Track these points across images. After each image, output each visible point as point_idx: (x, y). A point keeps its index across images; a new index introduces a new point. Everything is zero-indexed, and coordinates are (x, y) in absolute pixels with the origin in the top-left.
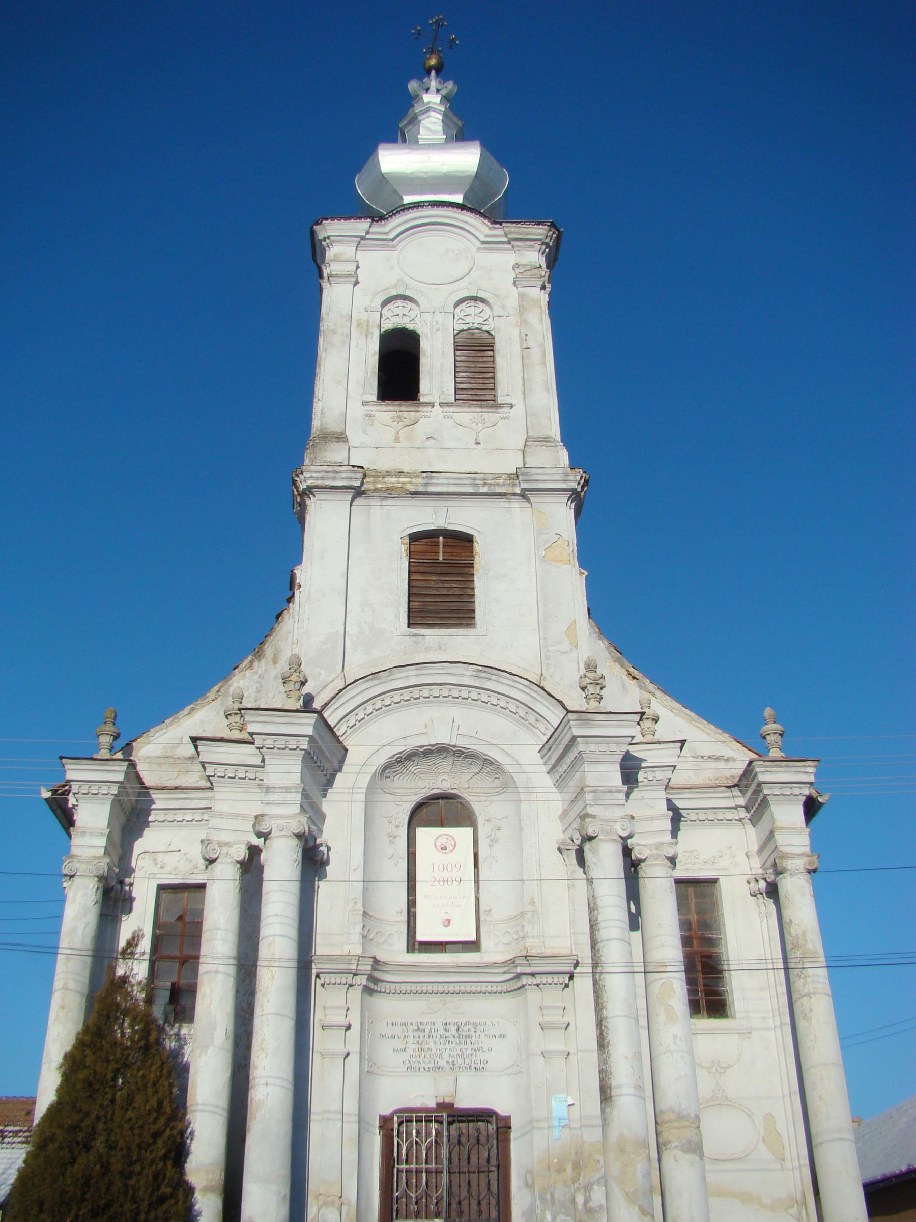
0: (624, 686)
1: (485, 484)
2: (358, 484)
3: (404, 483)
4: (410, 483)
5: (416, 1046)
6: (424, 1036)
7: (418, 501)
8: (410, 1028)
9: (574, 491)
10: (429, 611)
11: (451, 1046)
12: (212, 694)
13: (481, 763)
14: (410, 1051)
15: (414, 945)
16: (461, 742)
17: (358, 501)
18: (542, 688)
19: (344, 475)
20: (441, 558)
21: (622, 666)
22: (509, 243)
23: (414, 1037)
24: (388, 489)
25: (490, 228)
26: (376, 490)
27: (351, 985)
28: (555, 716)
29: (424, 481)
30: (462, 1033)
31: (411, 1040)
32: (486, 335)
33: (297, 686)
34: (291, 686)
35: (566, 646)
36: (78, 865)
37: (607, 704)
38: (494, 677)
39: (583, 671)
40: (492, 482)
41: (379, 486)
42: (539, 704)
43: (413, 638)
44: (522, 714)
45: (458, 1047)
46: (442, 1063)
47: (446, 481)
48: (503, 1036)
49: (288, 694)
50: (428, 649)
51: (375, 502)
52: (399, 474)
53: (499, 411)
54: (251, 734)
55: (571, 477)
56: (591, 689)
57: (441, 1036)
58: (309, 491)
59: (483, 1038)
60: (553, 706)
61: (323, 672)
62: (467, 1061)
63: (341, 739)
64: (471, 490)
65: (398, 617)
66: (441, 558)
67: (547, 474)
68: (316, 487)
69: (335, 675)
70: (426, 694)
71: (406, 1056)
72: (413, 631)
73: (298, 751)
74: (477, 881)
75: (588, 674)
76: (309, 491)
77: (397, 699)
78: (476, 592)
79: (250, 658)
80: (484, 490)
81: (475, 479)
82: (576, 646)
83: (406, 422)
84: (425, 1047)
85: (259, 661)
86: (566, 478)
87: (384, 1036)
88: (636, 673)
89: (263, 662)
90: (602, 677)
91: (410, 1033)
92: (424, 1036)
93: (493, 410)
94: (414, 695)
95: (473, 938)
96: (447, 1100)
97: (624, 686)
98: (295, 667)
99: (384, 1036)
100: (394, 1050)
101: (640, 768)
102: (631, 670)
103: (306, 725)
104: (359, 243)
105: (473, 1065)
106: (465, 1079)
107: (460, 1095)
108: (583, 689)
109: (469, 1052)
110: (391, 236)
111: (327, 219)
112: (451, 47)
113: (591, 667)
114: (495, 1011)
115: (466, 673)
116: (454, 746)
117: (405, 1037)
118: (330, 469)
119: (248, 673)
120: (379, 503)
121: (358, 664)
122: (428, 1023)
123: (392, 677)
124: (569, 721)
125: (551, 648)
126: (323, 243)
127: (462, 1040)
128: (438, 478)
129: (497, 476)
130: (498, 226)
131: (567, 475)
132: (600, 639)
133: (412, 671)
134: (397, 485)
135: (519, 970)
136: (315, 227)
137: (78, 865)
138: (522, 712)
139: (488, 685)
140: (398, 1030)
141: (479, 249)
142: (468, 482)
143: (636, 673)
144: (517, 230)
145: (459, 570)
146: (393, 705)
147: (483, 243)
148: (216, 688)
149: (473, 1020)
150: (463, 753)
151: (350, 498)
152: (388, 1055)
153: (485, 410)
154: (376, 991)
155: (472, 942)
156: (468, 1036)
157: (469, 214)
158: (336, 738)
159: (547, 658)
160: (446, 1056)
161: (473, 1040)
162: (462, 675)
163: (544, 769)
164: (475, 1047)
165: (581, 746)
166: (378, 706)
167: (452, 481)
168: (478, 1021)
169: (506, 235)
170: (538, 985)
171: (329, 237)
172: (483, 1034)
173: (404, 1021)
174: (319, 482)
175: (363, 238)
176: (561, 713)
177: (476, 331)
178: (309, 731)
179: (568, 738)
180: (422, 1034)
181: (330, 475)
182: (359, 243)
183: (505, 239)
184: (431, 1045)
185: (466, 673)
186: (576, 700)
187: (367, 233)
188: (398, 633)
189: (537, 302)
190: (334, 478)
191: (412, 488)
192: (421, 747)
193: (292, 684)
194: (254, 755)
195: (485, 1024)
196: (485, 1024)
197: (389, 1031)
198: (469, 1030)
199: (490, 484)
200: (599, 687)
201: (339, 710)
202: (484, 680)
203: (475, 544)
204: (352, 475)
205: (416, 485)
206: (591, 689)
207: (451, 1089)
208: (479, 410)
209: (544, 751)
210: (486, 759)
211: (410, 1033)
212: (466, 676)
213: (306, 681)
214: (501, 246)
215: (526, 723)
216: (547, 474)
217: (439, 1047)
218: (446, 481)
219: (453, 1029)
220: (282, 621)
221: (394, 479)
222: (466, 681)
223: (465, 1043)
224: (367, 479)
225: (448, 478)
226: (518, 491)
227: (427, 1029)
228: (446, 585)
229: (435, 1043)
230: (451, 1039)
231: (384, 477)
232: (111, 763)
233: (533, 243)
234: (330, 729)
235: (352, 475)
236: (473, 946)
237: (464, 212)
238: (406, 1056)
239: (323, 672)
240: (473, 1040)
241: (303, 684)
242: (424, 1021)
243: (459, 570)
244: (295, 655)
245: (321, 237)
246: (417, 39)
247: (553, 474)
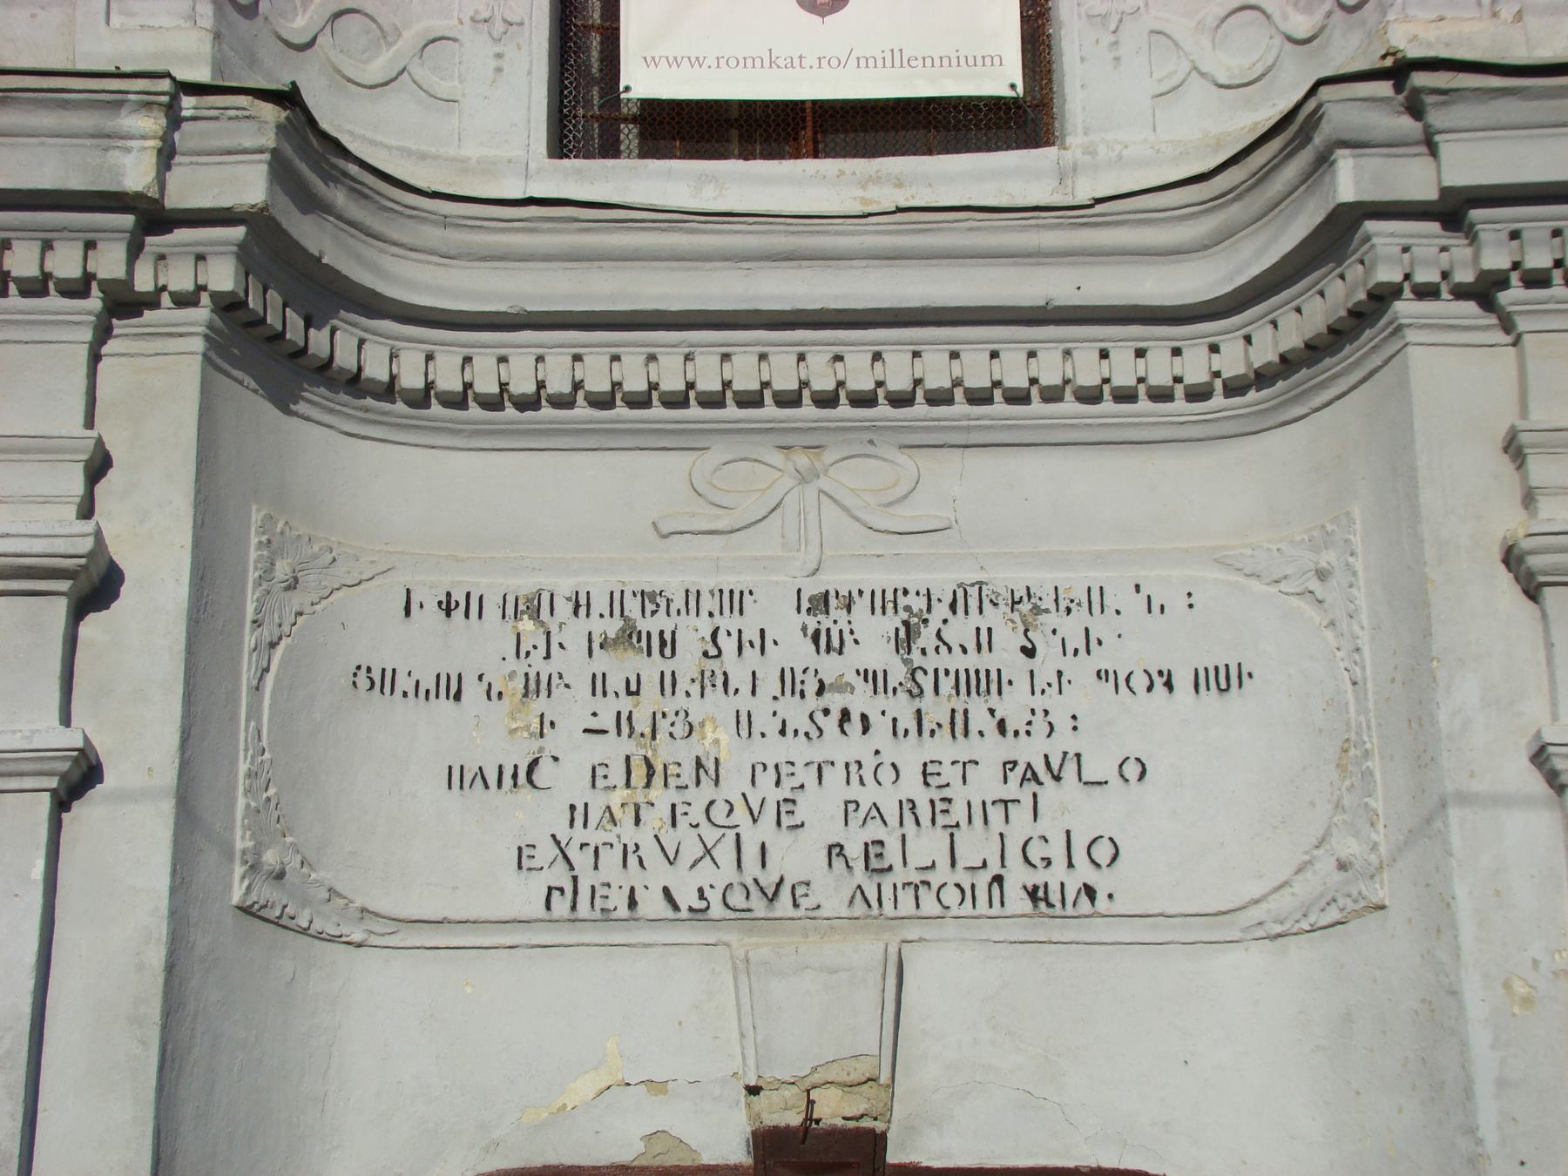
5: (613, 749)
6: (668, 684)
8: (573, 633)
11: (854, 746)
14: (566, 781)
15: (589, 108)
23: (598, 686)
27: (125, 303)
30: (938, 656)
31: (573, 708)
45: (910, 754)
46: (797, 858)
48: (1222, 680)
57: (789, 682)
59: (1084, 695)
62: (976, 845)
71: (537, 816)
84: (672, 752)
87: (384, 682)
91: (573, 663)
92: (668, 684)
95: (1002, 76)
96: (833, 1109)
99: (384, 682)
100: (456, 778)
105: (1018, 877)
106: (954, 977)
107: (922, 1076)
109: (986, 784)
114: (1169, 530)
117: (533, 687)
122: (692, 598)
127: (936, 710)
135: (1349, 181)
140: (484, 647)
149: (1006, 578)
152: (414, 818)
154: (324, 371)
155: (996, 105)
156: (976, 683)
160: (821, 810)
161: (1013, 706)
164: (1030, 751)
168: (1042, 580)
170: (1484, 291)
172: (1081, 670)
173: (524, 585)
180: (650, 668)
184: (719, 739)
195: (1096, 600)
196: (1096, 600)
197: (422, 648)
198: (984, 641)
207: (856, 1032)
211: (573, 663)
217: (775, 750)
219: (872, 640)
223: (959, 725)
227: (692, 633)
229: (744, 723)
230: (860, 700)
236: (1020, 120)
238: (537, 816)
240: (1013, 706)
242: (673, 584)
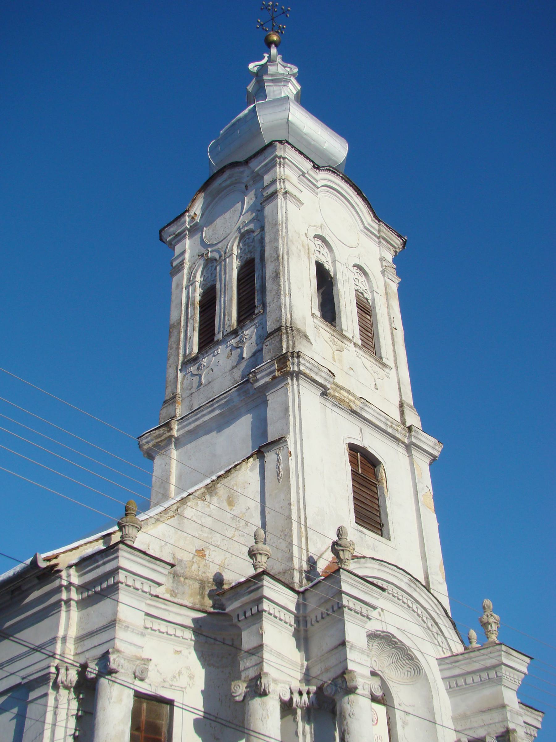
1: (391, 427)
4: (354, 402)
9: (435, 457)
19: (323, 375)
22: (378, 238)
25: (372, 220)
26: (334, 397)
29: (362, 405)
32: (365, 301)
36: (122, 661)
38: (418, 589)
40: (395, 427)
41: (337, 394)
51: (329, 405)
52: (349, 392)
53: (384, 369)
64: (383, 427)
76: (298, 374)
80: (390, 430)
81: (387, 419)
85: (211, 496)
86: (434, 446)
93: (381, 366)
115: (404, 579)
120: (330, 407)
128: (369, 407)
130: (377, 221)
131: (435, 444)
133: (375, 565)
134: (346, 400)
137: (122, 661)
141: (361, 230)
142: (383, 420)
144: (387, 232)
145: (369, 486)
147: (365, 228)
157: (361, 200)
162: (402, 580)
167: (375, 414)
169: (379, 231)
171: (284, 158)
174: (307, 372)
177: (360, 295)
181: (315, 369)
185: (404, 579)
190: (317, 374)
191: (354, 408)
199: (394, 428)
204: (328, 377)
205: (356, 405)
208: (374, 361)
212: (403, 582)
214: (373, 236)
221: (346, 394)
225: (374, 410)
226: (406, 441)
232: (158, 562)
233: (391, 247)
235: (328, 377)
237: (358, 196)
243: (369, 486)
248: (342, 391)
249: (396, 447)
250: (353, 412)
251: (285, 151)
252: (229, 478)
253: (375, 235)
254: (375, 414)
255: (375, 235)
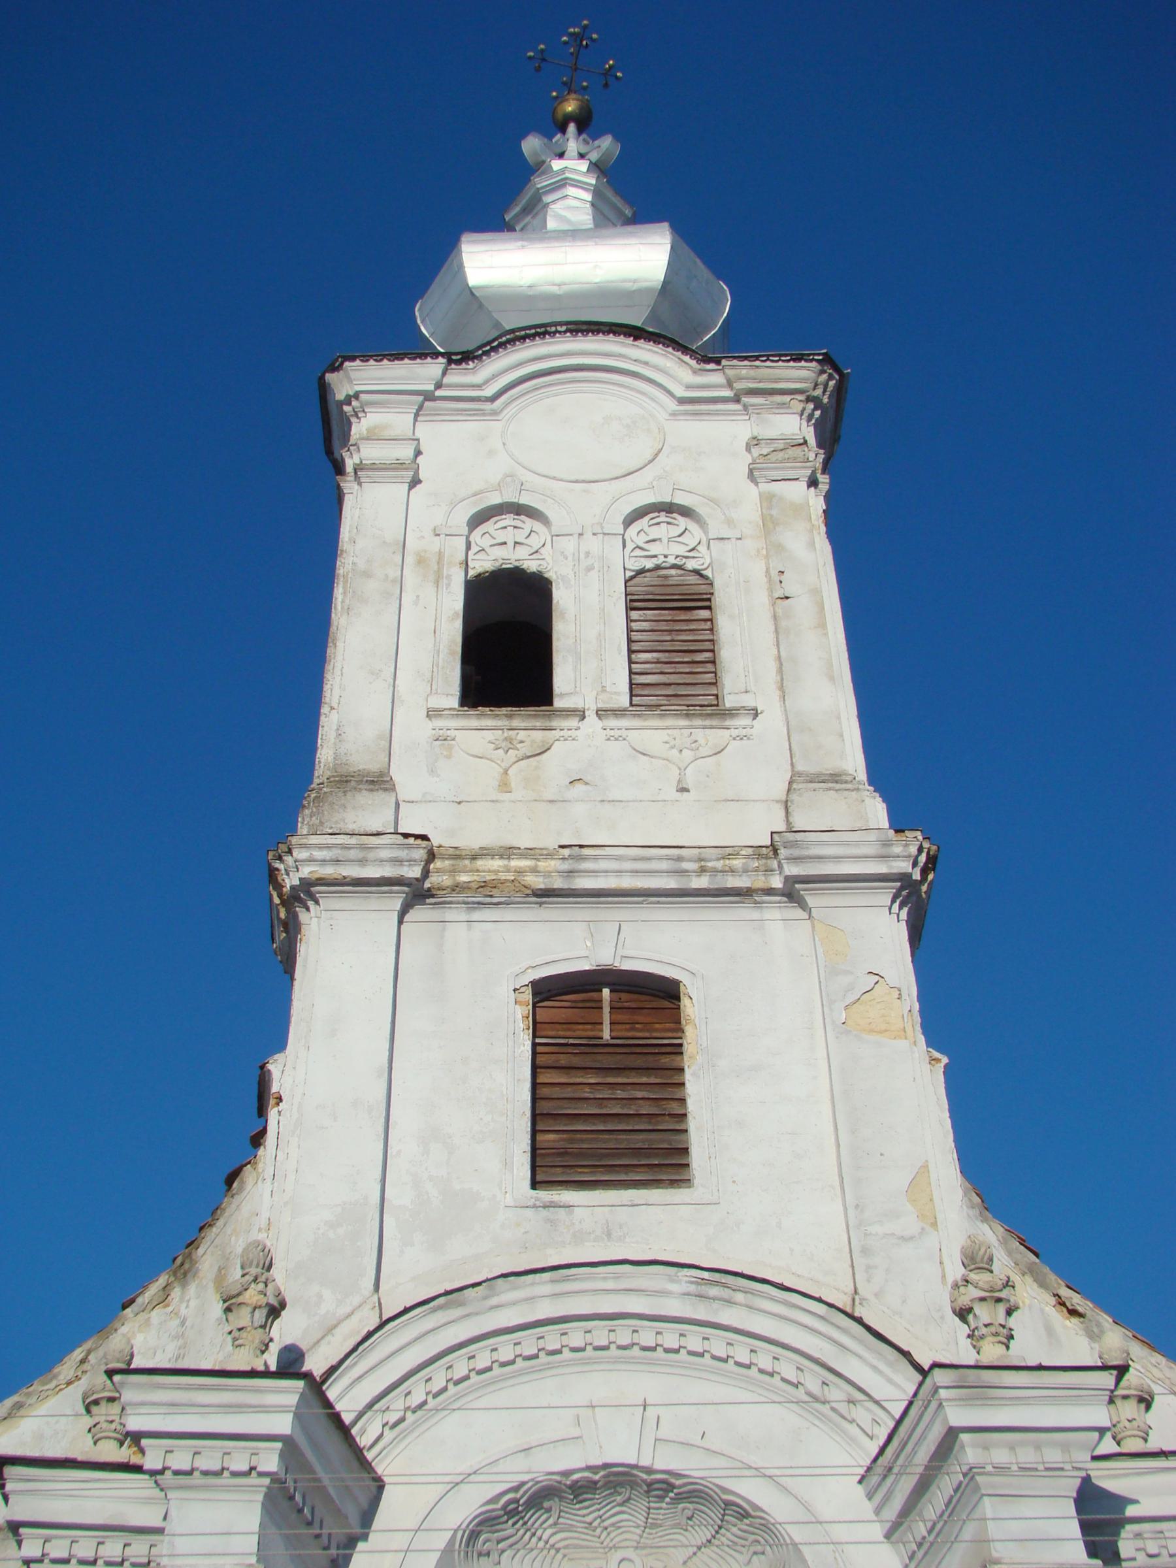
0: (1050, 1331)
1: (703, 870)
2: (415, 872)
3: (520, 872)
4: (534, 870)
7: (553, 912)
9: (904, 878)
10: (582, 1154)
12: (66, 1369)
13: (715, 1515)
16: (665, 1461)
17: (415, 914)
18: (859, 1321)
19: (385, 854)
20: (606, 1035)
21: (1042, 1284)
22: (736, 399)
24: (484, 885)
25: (695, 372)
26: (457, 888)
28: (894, 1386)
29: (566, 866)
32: (693, 579)
33: (260, 1316)
34: (243, 1317)
35: (909, 1222)
37: (1026, 1349)
38: (739, 1297)
39: (956, 1271)
40: (719, 865)
41: (464, 878)
42: (855, 1362)
43: (544, 1213)
44: (813, 1385)
47: (614, 865)
49: (236, 1336)
50: (579, 1238)
52: (508, 852)
53: (728, 723)
54: (136, 1438)
55: (897, 850)
56: (983, 1313)
58: (306, 892)
60: (890, 1364)
61: (327, 1294)
63: (369, 1456)
64: (671, 883)
65: (507, 1164)
66: (606, 1035)
67: (847, 843)
68: (321, 882)
69: (356, 1300)
70: (576, 1340)
72: (544, 1195)
73: (253, 1480)
74: (853, 1267)
75: (973, 1276)
76: (306, 892)
77: (506, 1354)
78: (692, 1105)
79: (162, 1280)
80: (702, 882)
81: (680, 859)
82: (934, 1224)
83: (524, 749)
85: (184, 1286)
86: (884, 851)
88: (1075, 1300)
89: (192, 1289)
90: (1008, 1284)
93: (715, 722)
94: (545, 1342)
97: (1050, 1331)
98: (254, 1271)
101: (1119, 1524)
102: (1065, 1292)
103: (276, 1409)
104: (421, 408)
108: (963, 1314)
110: (489, 392)
111: (353, 359)
112: (606, 85)
113: (976, 1260)
115: (674, 1287)
116: (649, 1470)
118: (353, 841)
119: (156, 1315)
120: (463, 916)
121: (411, 1273)
123: (494, 1301)
124: (936, 1389)
125: (875, 1229)
126: (346, 408)
128: (596, 858)
129: (727, 852)
130: (712, 366)
132: (985, 1220)
133: (542, 1285)
134: (503, 876)
136: (329, 377)
138: (812, 1380)
139: (727, 1316)
141: (674, 414)
142: (664, 865)
143: (1075, 1300)
144: (752, 373)
145: (650, 1061)
146: (497, 1371)
147: (682, 401)
148: (78, 1354)
150: (672, 1487)
151: (397, 904)
153: (698, 722)
157: (650, 346)
158: (358, 1453)
159: (865, 1251)
163: (877, 1531)
165: (970, 1451)
166: (460, 1370)
167: (628, 865)
169: (730, 384)
171: (356, 396)
174: (328, 871)
175: (429, 397)
176: (908, 1381)
177: (673, 572)
178: (283, 1424)
179: (936, 1434)
181: (352, 854)
182: (421, 408)
183: (728, 393)
186: (944, 1341)
187: (439, 386)
188: (509, 1200)
189: (800, 510)
190: (362, 862)
191: (539, 883)
192: (566, 1473)
193: (245, 1312)
194: (148, 1501)
199: (715, 871)
200: (1001, 1309)
201: (364, 1383)
202: (716, 1305)
203: (685, 1001)
204: (403, 854)
205: (547, 874)
206: (983, 1313)
208: (683, 722)
209: (874, 1479)
210: (727, 1504)
212: (673, 1296)
213: (283, 1305)
215: (825, 1409)
216: (847, 843)
218: (614, 865)
220: (241, 1189)
221: (497, 863)
222: (674, 1308)
224: (437, 864)
225: (618, 858)
226: (777, 882)
228: (620, 1094)
231: (474, 858)
233: (787, 398)
234: (343, 1430)
235: (403, 854)
237: (641, 343)
239: (327, 1294)
241: (275, 1311)
243: (650, 1061)
244: (257, 1243)
245: (340, 396)
246: (538, 69)
247: (857, 843)
248: (479, 863)
249: (755, 915)
250: (545, 894)
251: (350, 381)
252: (220, 1223)
253: (724, 400)
254: (628, 865)
255: (724, 400)
